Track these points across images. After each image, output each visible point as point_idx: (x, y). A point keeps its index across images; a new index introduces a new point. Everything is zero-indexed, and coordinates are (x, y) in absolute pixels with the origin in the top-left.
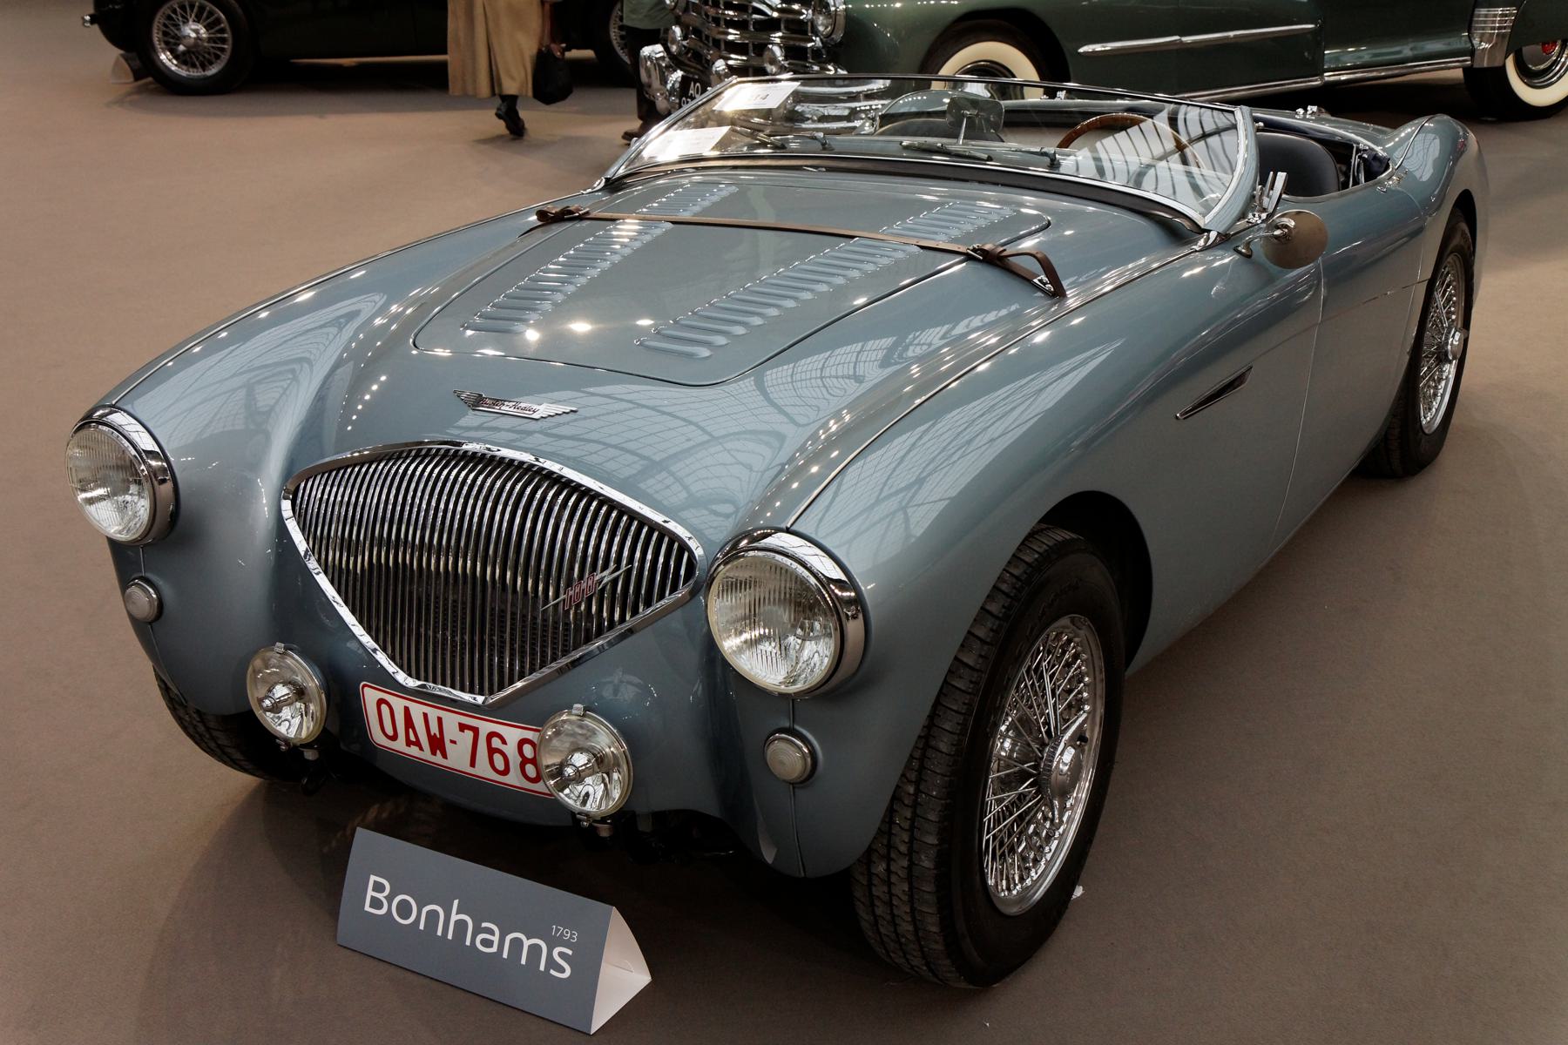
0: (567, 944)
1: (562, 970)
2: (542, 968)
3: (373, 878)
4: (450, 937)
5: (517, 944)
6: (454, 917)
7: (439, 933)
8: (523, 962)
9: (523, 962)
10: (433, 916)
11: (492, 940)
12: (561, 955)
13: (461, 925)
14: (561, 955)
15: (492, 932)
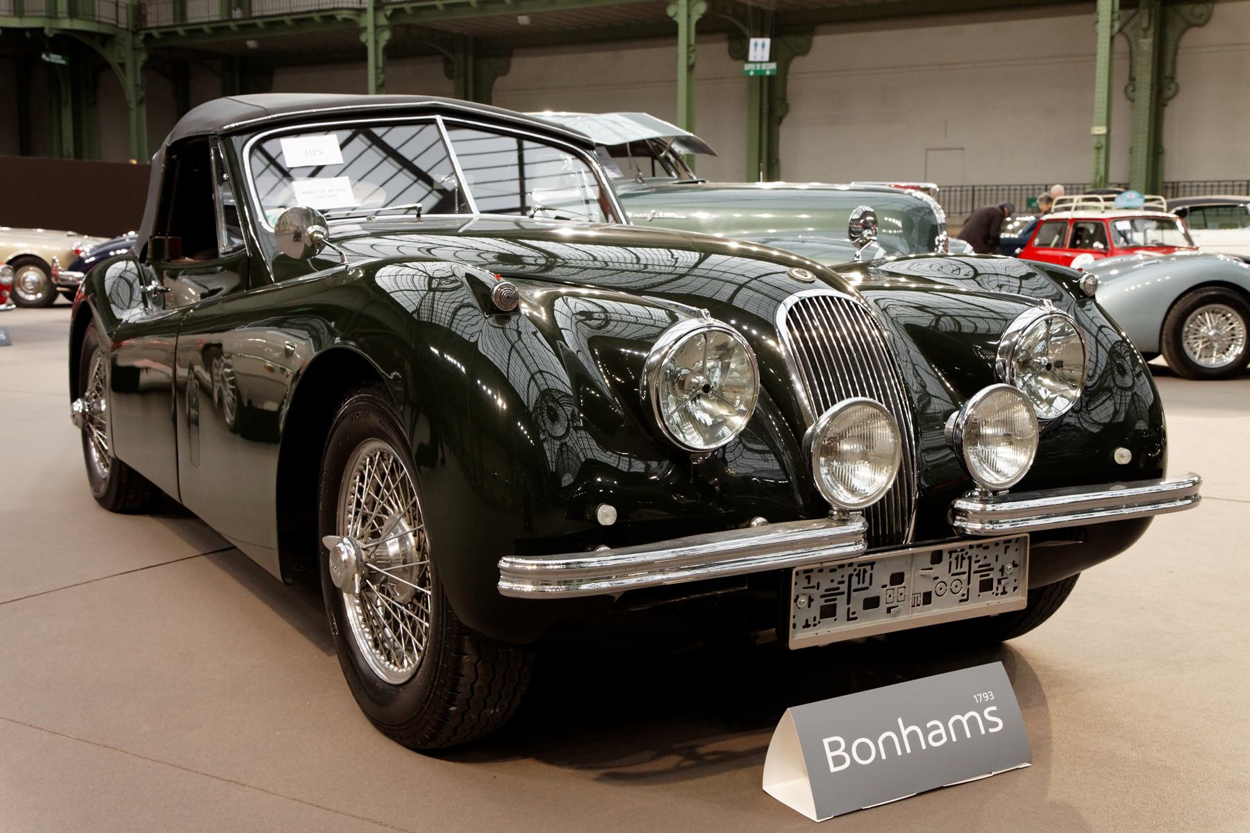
0: (990, 704)
1: (996, 725)
2: (983, 732)
3: (826, 741)
4: (909, 751)
5: (958, 724)
6: (905, 733)
7: (899, 753)
8: (969, 736)
9: (969, 736)
10: (888, 741)
11: (939, 734)
12: (991, 713)
13: (913, 736)
14: (991, 713)
15: (936, 727)
